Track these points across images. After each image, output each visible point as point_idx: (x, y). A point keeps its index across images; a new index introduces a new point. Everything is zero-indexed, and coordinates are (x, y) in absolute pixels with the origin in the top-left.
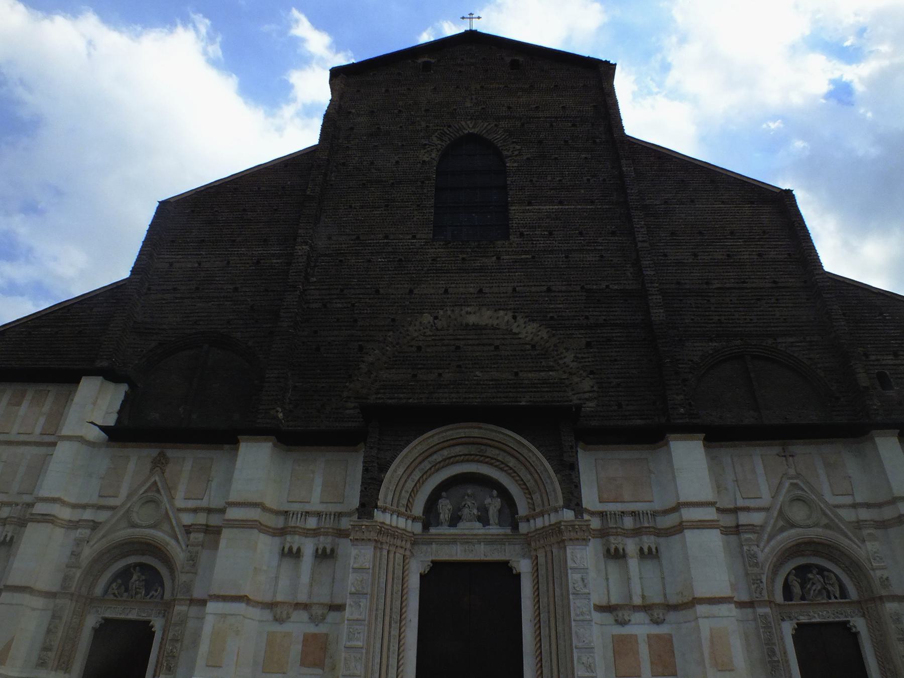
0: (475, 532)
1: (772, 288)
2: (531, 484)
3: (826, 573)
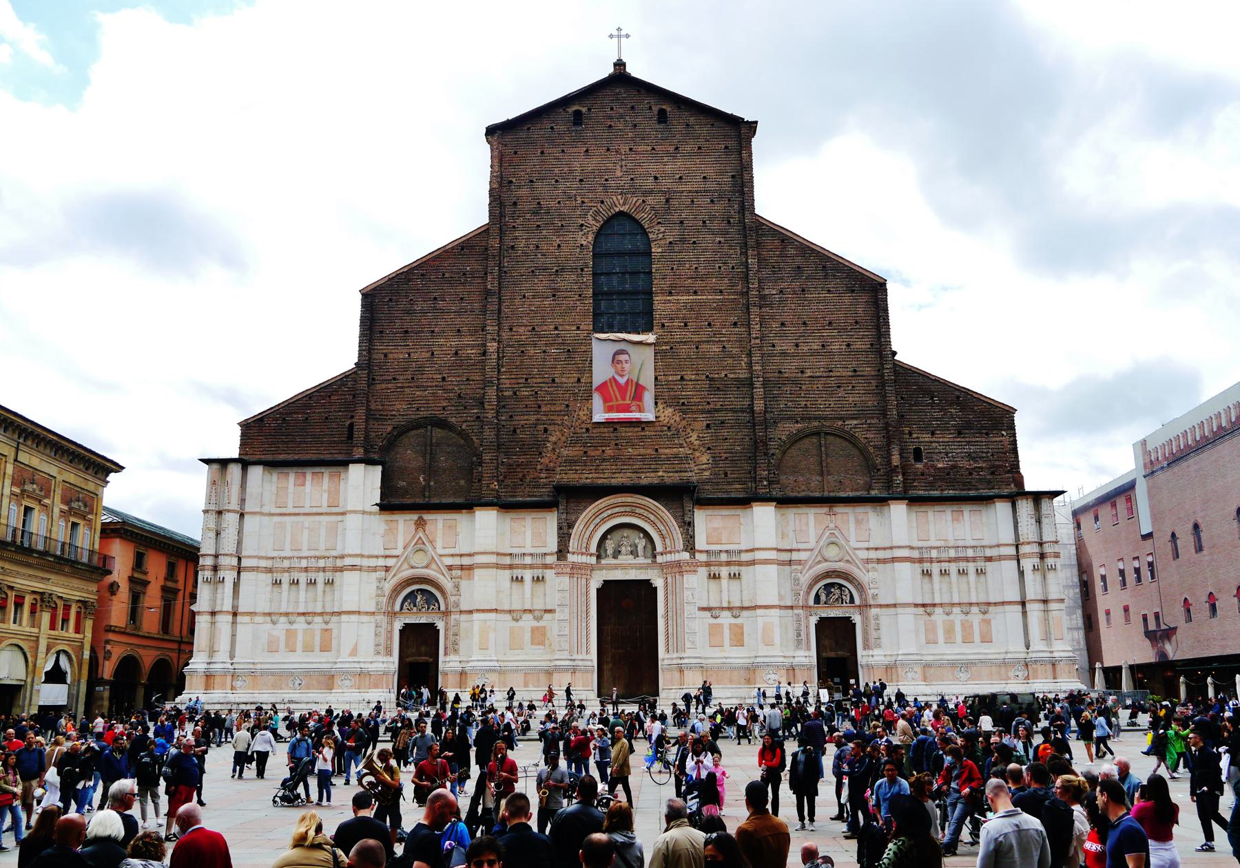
0: (630, 562)
1: (852, 376)
2: (664, 532)
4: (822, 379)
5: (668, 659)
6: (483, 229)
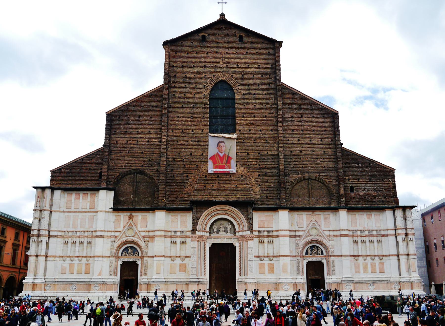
0: (224, 235)
1: (323, 154)
2: (239, 222)
3: (318, 248)
4: (310, 155)
5: (241, 279)
6: (161, 87)
